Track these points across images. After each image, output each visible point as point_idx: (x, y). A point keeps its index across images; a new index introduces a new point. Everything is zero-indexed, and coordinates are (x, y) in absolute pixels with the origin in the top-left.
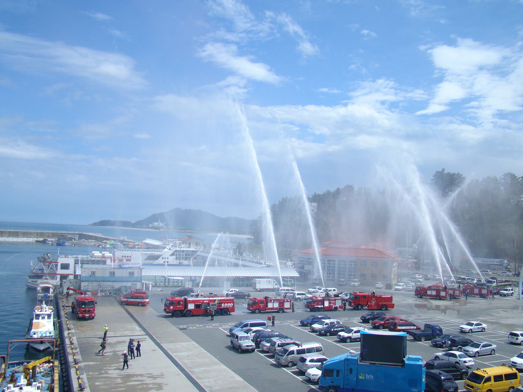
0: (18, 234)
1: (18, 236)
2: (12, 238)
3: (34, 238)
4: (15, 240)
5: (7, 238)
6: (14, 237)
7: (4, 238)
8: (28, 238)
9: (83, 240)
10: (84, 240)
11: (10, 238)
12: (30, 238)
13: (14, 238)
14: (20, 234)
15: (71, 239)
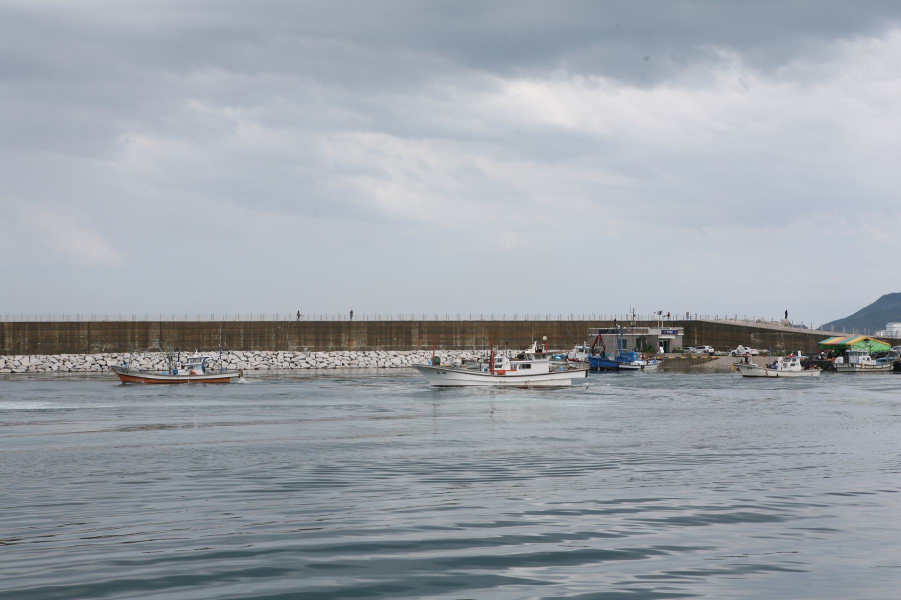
0: (409, 334)
1: (410, 343)
2: (383, 354)
3: (477, 349)
4: (397, 361)
5: (359, 353)
6: (391, 349)
7: (347, 353)
8: (452, 352)
9: (707, 348)
10: (712, 350)
11: (373, 354)
12: (463, 348)
13: (393, 353)
14: (415, 332)
15: (647, 347)
